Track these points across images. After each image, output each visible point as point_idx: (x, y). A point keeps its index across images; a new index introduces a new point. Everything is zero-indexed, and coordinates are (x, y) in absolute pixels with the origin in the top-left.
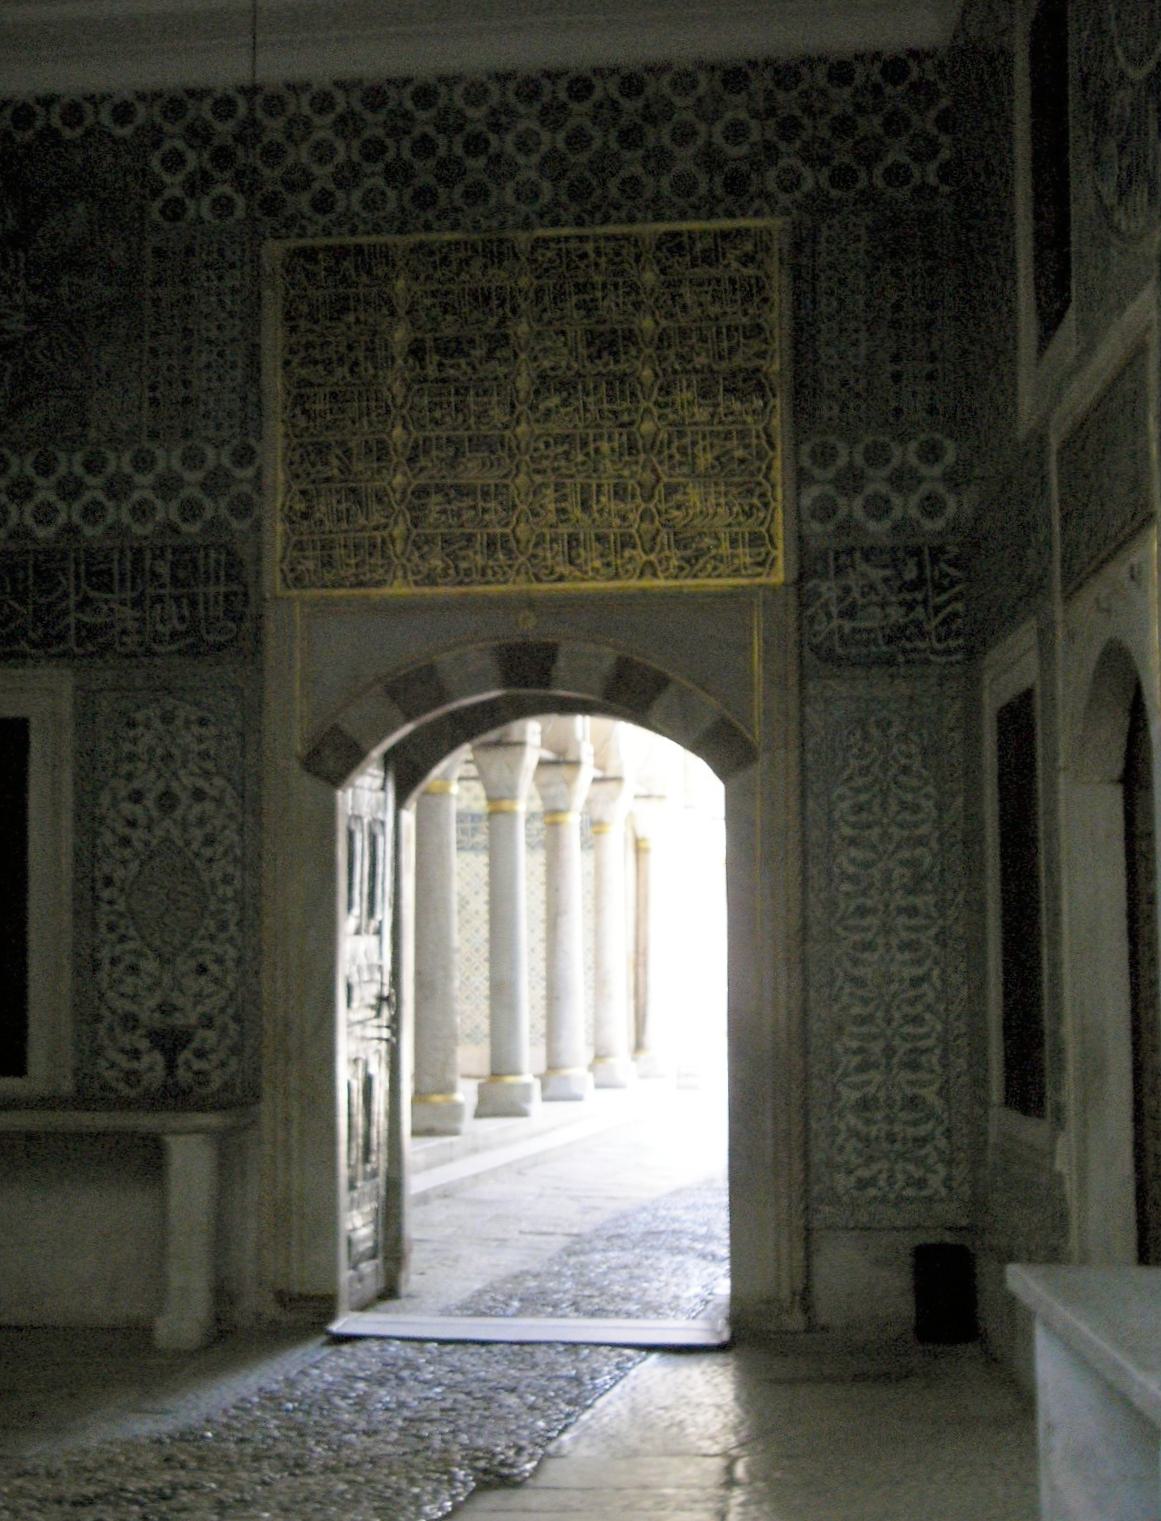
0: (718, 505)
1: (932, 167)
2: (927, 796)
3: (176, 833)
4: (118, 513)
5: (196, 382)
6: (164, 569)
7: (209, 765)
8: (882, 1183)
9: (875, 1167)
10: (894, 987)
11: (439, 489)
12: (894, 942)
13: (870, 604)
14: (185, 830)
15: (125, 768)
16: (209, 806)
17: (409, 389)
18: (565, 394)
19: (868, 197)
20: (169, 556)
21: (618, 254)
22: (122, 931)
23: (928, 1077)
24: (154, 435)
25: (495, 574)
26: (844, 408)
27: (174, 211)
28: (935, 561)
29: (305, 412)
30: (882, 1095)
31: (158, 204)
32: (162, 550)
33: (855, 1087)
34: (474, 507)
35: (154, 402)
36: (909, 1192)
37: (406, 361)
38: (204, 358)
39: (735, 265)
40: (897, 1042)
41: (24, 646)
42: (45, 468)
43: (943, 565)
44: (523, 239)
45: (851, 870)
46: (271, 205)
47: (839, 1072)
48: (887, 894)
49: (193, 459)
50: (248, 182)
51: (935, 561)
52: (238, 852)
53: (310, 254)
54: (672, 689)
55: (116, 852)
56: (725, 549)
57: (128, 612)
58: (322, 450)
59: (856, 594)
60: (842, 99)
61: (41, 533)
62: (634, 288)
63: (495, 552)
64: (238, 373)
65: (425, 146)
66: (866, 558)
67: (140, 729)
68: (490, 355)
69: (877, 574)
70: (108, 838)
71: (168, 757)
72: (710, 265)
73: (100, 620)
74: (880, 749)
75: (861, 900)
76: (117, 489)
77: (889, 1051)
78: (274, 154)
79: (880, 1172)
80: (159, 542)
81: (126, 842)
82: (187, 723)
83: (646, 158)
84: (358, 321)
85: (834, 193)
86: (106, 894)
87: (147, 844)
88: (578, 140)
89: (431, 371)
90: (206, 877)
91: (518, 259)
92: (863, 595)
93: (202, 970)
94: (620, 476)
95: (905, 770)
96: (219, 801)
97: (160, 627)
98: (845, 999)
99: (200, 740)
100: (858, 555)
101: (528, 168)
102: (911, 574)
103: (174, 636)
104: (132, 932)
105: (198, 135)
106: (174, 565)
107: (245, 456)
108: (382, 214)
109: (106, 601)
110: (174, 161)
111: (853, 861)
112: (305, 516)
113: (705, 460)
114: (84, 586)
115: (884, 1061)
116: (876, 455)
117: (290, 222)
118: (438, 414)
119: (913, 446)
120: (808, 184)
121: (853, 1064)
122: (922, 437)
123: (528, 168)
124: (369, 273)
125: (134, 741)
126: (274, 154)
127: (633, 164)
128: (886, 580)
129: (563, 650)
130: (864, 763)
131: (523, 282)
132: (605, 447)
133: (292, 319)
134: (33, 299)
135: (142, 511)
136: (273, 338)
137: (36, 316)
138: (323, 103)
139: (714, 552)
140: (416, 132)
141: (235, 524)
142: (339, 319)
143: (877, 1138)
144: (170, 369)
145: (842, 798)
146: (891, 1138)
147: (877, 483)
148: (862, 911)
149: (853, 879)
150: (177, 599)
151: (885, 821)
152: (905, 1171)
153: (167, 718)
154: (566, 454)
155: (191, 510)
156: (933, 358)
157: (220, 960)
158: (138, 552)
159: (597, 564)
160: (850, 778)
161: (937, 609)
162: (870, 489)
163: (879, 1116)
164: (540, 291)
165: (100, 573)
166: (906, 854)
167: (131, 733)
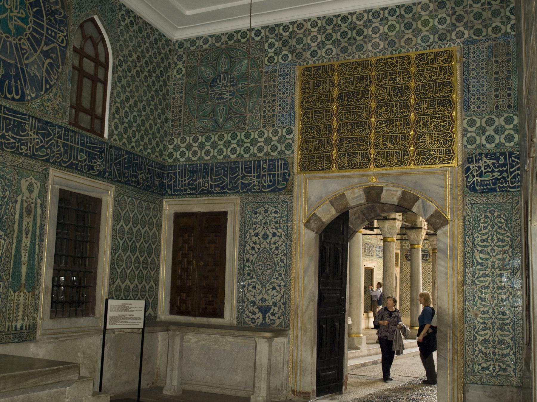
0: (436, 141)
2: (508, 237)
3: (267, 246)
4: (254, 150)
5: (276, 110)
6: (266, 166)
7: (277, 225)
8: (490, 369)
9: (489, 363)
10: (495, 302)
11: (347, 139)
12: (496, 286)
13: (488, 172)
14: (270, 245)
15: (254, 226)
16: (277, 238)
17: (338, 108)
18: (386, 108)
19: (487, 38)
20: (268, 162)
21: (403, 62)
22: (251, 275)
23: (507, 333)
24: (264, 127)
25: (363, 165)
26: (479, 107)
27: (271, 60)
28: (510, 157)
29: (307, 117)
30: (491, 339)
31: (267, 58)
32: (266, 160)
33: (481, 335)
34: (357, 144)
35: (264, 117)
36: (501, 373)
37: (337, 100)
38: (279, 103)
39: (441, 63)
40: (496, 321)
41: (226, 189)
42: (234, 136)
43: (513, 158)
45: (480, 261)
46: (299, 56)
47: (476, 330)
48: (493, 270)
49: (275, 133)
51: (510, 157)
52: (285, 252)
54: (420, 201)
55: (250, 251)
57: (256, 179)
59: (483, 169)
61: (232, 156)
62: (409, 73)
63: (364, 158)
64: (289, 106)
65: (344, 34)
66: (486, 157)
67: (258, 215)
69: (490, 162)
70: (248, 247)
71: (266, 223)
72: (433, 64)
73: (247, 182)
74: (491, 220)
75: (484, 272)
77: (493, 323)
79: (490, 365)
80: (264, 159)
81: (253, 248)
82: (272, 213)
83: (413, 31)
84: (323, 89)
85: (475, 38)
86: (247, 264)
87: (259, 249)
88: (392, 28)
89: (345, 102)
90: (275, 260)
91: (372, 66)
92: (485, 169)
93: (274, 288)
94: (404, 133)
95: (500, 228)
96: (280, 237)
97: (265, 184)
98: (478, 305)
99: (275, 218)
100: (483, 156)
101: (376, 37)
102: (502, 161)
103: (269, 186)
104: (254, 276)
105: (279, 37)
106: (269, 165)
107: (290, 131)
108: (331, 56)
109: (250, 176)
110: (271, 45)
111: (481, 258)
114: (243, 172)
115: (491, 327)
116: (490, 122)
117: (304, 61)
118: (346, 116)
119: (502, 119)
120: (466, 36)
121: (481, 328)
122: (506, 115)
124: (326, 74)
125: (256, 218)
126: (300, 41)
127: (408, 34)
128: (493, 164)
129: (385, 188)
130: (486, 225)
131: (374, 74)
133: (304, 89)
134: (232, 88)
135: (261, 149)
137: (233, 94)
139: (434, 156)
141: (286, 152)
142: (317, 89)
143: (489, 353)
144: (269, 106)
145: (478, 237)
146: (494, 353)
147: (490, 131)
148: (485, 276)
149: (481, 264)
150: (270, 175)
151: (493, 245)
152: (499, 366)
153: (266, 211)
154: (386, 126)
155: (274, 148)
156: (509, 89)
157: (279, 285)
158: (259, 162)
159: (396, 161)
160: (480, 230)
161: (511, 173)
162: (487, 134)
163: (490, 346)
165: (247, 168)
166: (500, 256)
167: (256, 216)
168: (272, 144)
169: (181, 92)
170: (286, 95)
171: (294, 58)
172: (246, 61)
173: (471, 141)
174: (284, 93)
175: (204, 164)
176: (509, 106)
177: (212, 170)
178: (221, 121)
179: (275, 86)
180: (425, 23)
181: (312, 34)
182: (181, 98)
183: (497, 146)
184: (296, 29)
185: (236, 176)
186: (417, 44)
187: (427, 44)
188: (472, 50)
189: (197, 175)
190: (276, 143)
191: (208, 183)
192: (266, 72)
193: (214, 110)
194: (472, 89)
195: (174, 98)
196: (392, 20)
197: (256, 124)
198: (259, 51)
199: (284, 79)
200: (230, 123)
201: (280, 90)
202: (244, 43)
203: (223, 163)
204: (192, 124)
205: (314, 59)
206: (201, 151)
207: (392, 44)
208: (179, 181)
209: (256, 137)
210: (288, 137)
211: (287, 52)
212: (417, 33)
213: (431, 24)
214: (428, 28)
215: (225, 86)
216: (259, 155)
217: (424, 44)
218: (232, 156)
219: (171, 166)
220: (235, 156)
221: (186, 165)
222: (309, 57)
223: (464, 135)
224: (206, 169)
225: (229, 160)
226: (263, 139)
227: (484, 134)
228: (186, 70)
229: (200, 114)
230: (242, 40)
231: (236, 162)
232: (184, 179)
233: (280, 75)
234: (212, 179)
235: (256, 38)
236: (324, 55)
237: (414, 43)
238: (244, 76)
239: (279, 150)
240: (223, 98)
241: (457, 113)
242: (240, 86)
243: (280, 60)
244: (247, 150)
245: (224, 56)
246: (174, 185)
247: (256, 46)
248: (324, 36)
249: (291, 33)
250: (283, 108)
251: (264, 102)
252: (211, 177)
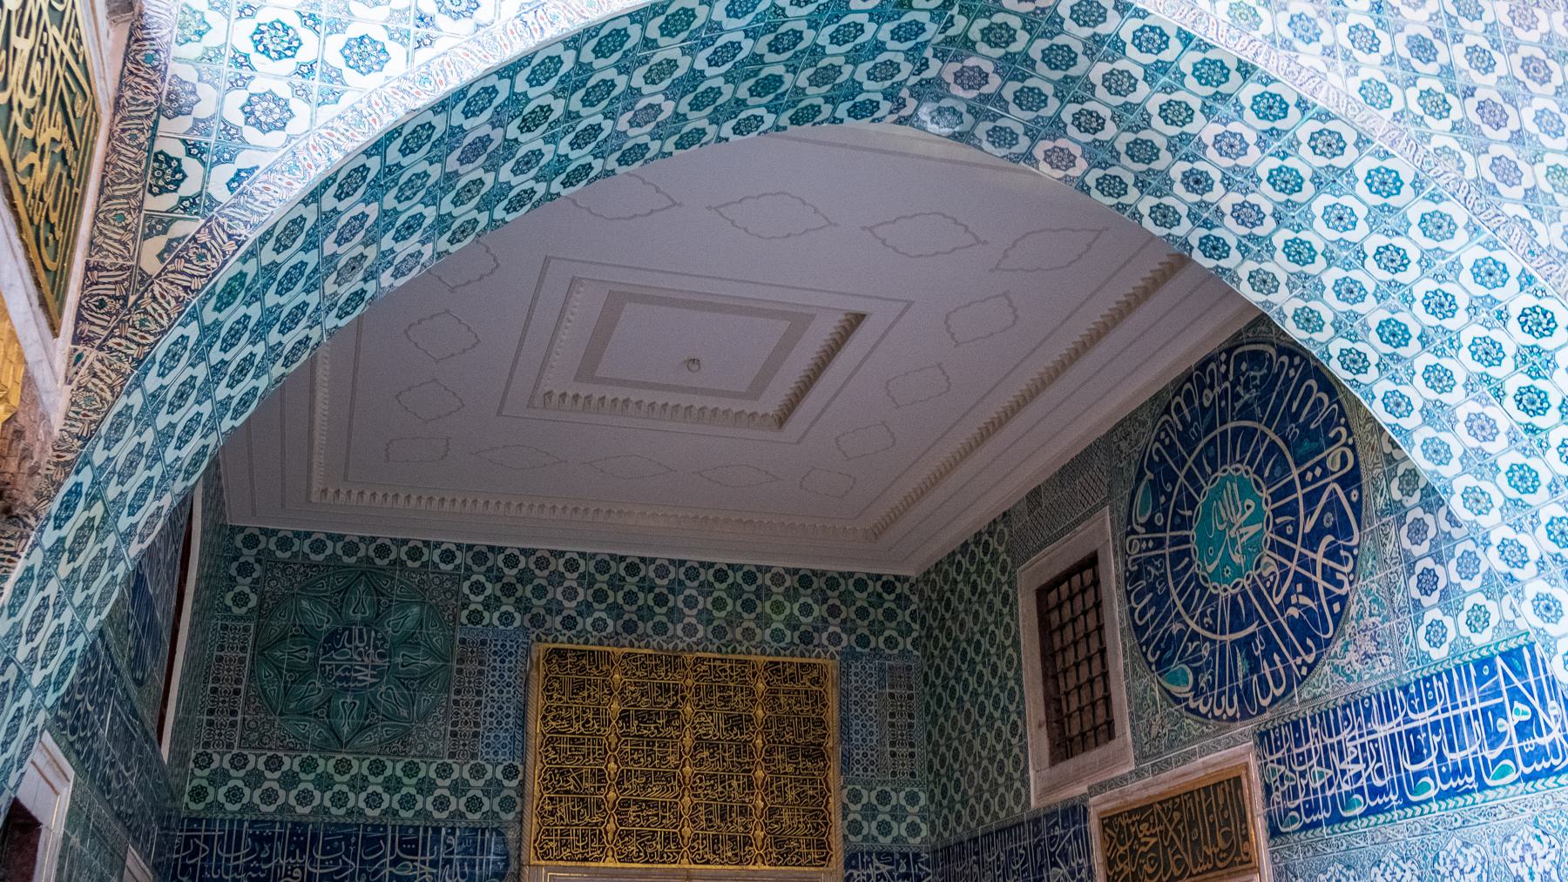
1: (909, 640)
24: (452, 755)
26: (865, 770)
27: (475, 618)
28: (915, 862)
31: (465, 613)
32: (453, 829)
35: (454, 734)
38: (489, 710)
44: (689, 657)
46: (537, 621)
49: (478, 772)
50: (523, 606)
51: (915, 862)
53: (561, 653)
56: (804, 850)
57: (427, 869)
58: (563, 773)
60: (861, 598)
62: (752, 692)
64: (511, 720)
65: (630, 597)
68: (668, 723)
69: (885, 869)
76: (426, 787)
78: (540, 591)
85: (858, 649)
88: (719, 604)
89: (633, 729)
101: (690, 616)
102: (903, 870)
110: (478, 588)
112: (552, 814)
113: (791, 795)
116: (884, 798)
119: (902, 794)
123: (690, 616)
127: (749, 621)
128: (890, 872)
131: (689, 682)
132: (734, 783)
134: (378, 662)
136: (537, 702)
138: (572, 565)
140: (626, 589)
156: (912, 745)
158: (437, 830)
162: (880, 818)
164: (698, 688)
165: (406, 842)
168: (470, 794)
169: (243, 649)
170: (505, 695)
171: (527, 624)
172: (416, 609)
173: (855, 828)
174: (501, 692)
175: (295, 824)
176: (913, 775)
177: (315, 837)
178: (346, 729)
179: (481, 673)
180: (778, 607)
181: (566, 584)
182: (242, 660)
183: (895, 840)
184: (532, 566)
185: (379, 859)
186: (763, 641)
187: (783, 645)
188: (853, 670)
189: (271, 849)
190: (479, 794)
191: (302, 869)
192: (463, 641)
193: (329, 700)
194: (854, 736)
195: (220, 659)
196: (720, 590)
197: (434, 748)
198: (449, 595)
199: (503, 661)
200: (369, 739)
201: (493, 684)
202: (413, 570)
203: (346, 825)
204: (267, 726)
205: (568, 633)
206: (288, 791)
207: (719, 632)
208: (219, 858)
209: (433, 775)
210: (506, 783)
211: (511, 609)
212: (763, 621)
213: (787, 612)
214: (782, 617)
215: (360, 654)
216: (436, 815)
217: (775, 645)
218: (369, 812)
219: (199, 821)
220: (377, 812)
221: (241, 822)
222: (559, 627)
223: (845, 817)
224: (299, 836)
225: (362, 820)
226: (448, 782)
227: (874, 817)
228: (260, 605)
229: (292, 706)
230: (410, 564)
231: (379, 826)
232: (232, 855)
233: (495, 653)
234: (312, 860)
235: (443, 566)
236: (590, 628)
237: (758, 638)
238: (409, 641)
239: (485, 809)
240: (356, 679)
241: (834, 777)
242: (400, 660)
243: (496, 622)
244: (407, 802)
245: (362, 588)
246: (202, 868)
247: (442, 582)
248: (591, 592)
249: (522, 572)
250: (499, 723)
251: (456, 702)
252: (311, 855)
